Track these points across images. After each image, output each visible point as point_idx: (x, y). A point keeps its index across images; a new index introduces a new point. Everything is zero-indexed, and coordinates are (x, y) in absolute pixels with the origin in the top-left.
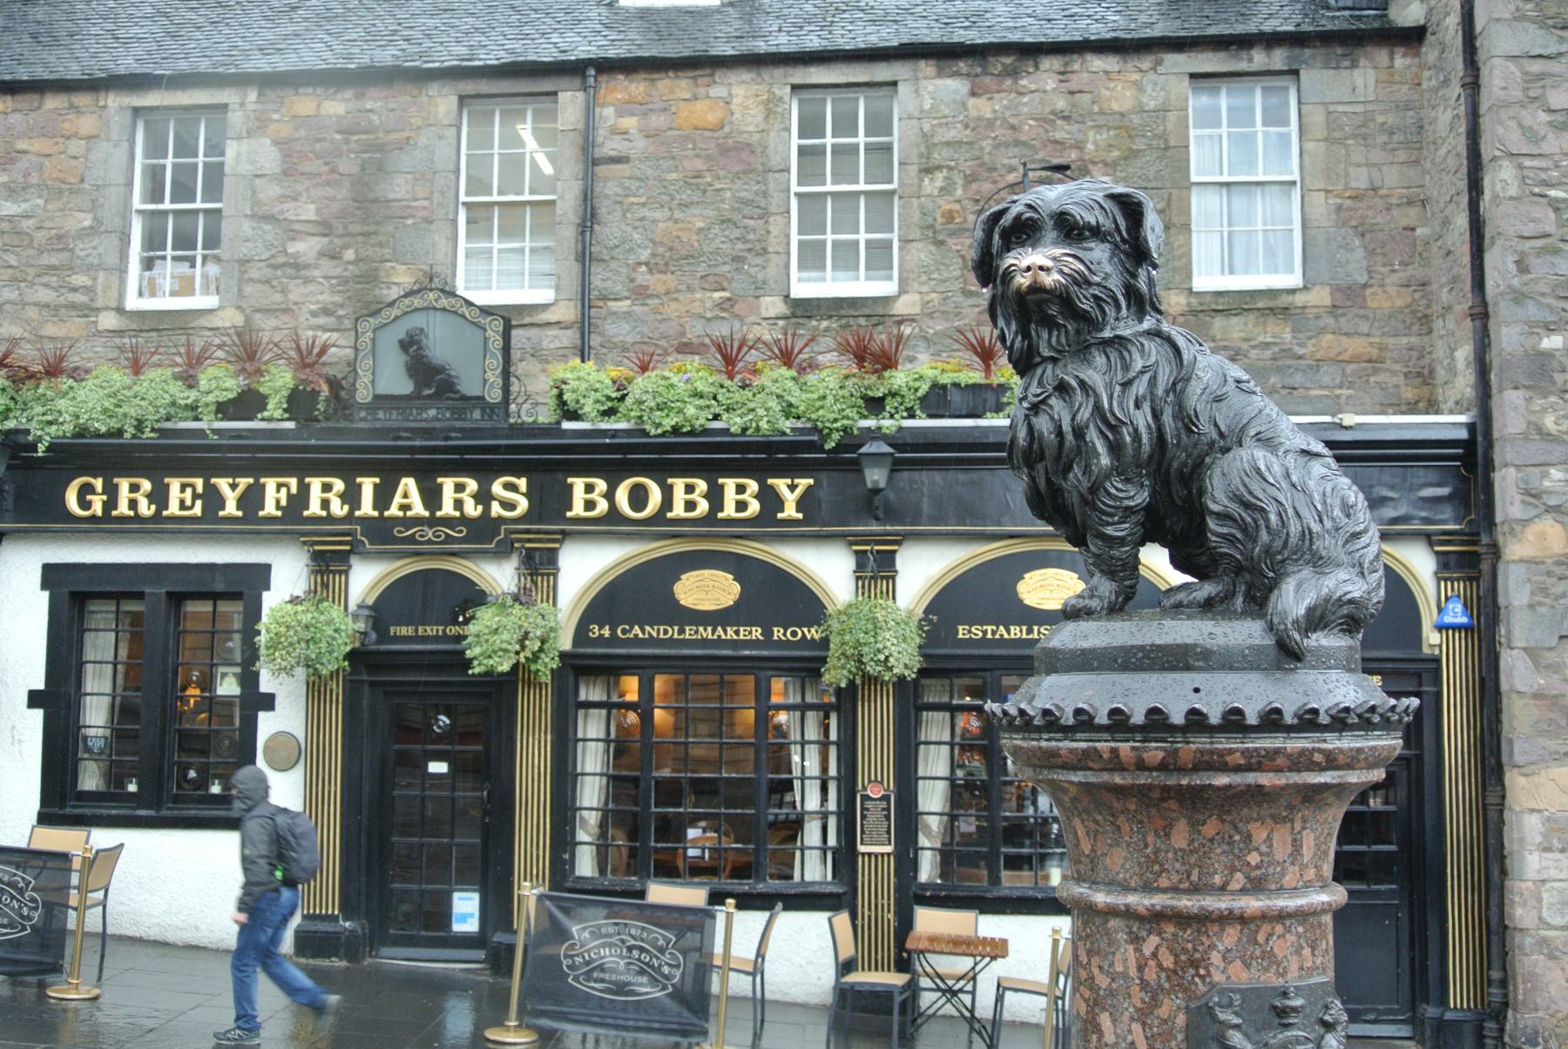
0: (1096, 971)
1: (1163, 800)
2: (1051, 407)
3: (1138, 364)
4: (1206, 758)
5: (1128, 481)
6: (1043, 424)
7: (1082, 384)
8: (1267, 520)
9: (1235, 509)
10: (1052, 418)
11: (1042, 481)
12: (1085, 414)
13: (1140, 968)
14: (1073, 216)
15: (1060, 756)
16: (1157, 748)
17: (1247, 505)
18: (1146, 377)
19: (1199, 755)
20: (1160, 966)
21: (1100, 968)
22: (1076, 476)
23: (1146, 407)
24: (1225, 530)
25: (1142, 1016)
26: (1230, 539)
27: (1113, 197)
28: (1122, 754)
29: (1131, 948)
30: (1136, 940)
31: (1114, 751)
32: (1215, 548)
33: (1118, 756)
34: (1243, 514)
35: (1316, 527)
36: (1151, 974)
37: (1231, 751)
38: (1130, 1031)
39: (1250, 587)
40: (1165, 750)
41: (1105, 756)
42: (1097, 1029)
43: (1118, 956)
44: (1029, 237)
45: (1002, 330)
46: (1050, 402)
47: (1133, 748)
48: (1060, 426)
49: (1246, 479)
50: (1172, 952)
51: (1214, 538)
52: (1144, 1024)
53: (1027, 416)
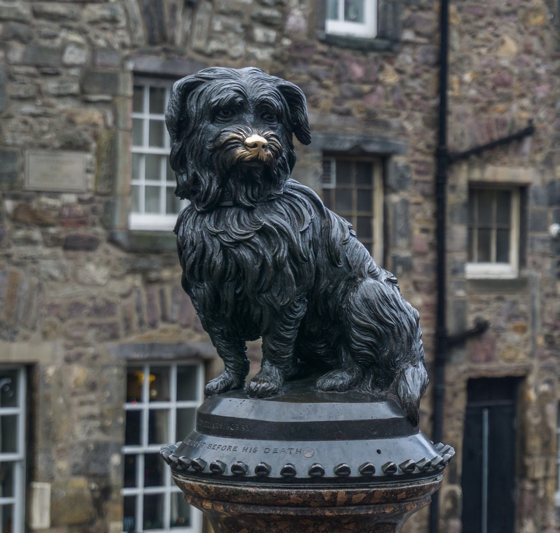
1: (348, 523)
2: (255, 244)
3: (308, 218)
4: (388, 496)
5: (299, 301)
6: (246, 254)
7: (280, 230)
8: (393, 332)
9: (374, 324)
10: (256, 254)
11: (228, 294)
12: (284, 253)
14: (272, 105)
15: (289, 499)
16: (362, 492)
17: (381, 322)
18: (311, 227)
19: (385, 494)
22: (273, 297)
23: (312, 249)
26: (370, 346)
27: (281, 88)
28: (339, 496)
31: (334, 495)
32: (360, 350)
33: (337, 497)
34: (379, 327)
35: (411, 335)
37: (402, 490)
39: (376, 376)
40: (367, 492)
41: (326, 498)
44: (234, 114)
45: (195, 174)
46: (253, 240)
47: (347, 493)
48: (264, 261)
49: (381, 304)
51: (359, 344)
53: (223, 248)
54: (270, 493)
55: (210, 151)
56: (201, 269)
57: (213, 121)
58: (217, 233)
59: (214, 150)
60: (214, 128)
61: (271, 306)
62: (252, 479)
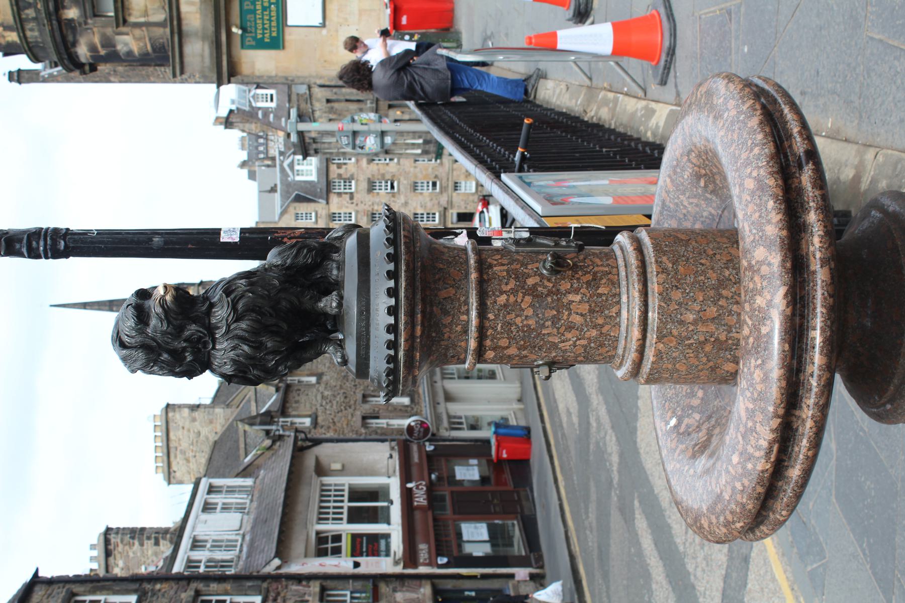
0: (509, 287)
2: (235, 297)
13: (503, 265)
20: (500, 259)
21: (507, 284)
24: (305, 251)
25: (525, 265)
26: (310, 250)
28: (406, 234)
29: (495, 269)
30: (491, 266)
31: (405, 236)
36: (505, 262)
38: (532, 269)
42: (535, 286)
43: (499, 274)
50: (495, 255)
52: (527, 264)
54: (405, 271)
55: (168, 326)
56: (252, 342)
57: (147, 324)
58: (227, 325)
59: (169, 323)
60: (153, 322)
61: (280, 291)
62: (396, 283)
